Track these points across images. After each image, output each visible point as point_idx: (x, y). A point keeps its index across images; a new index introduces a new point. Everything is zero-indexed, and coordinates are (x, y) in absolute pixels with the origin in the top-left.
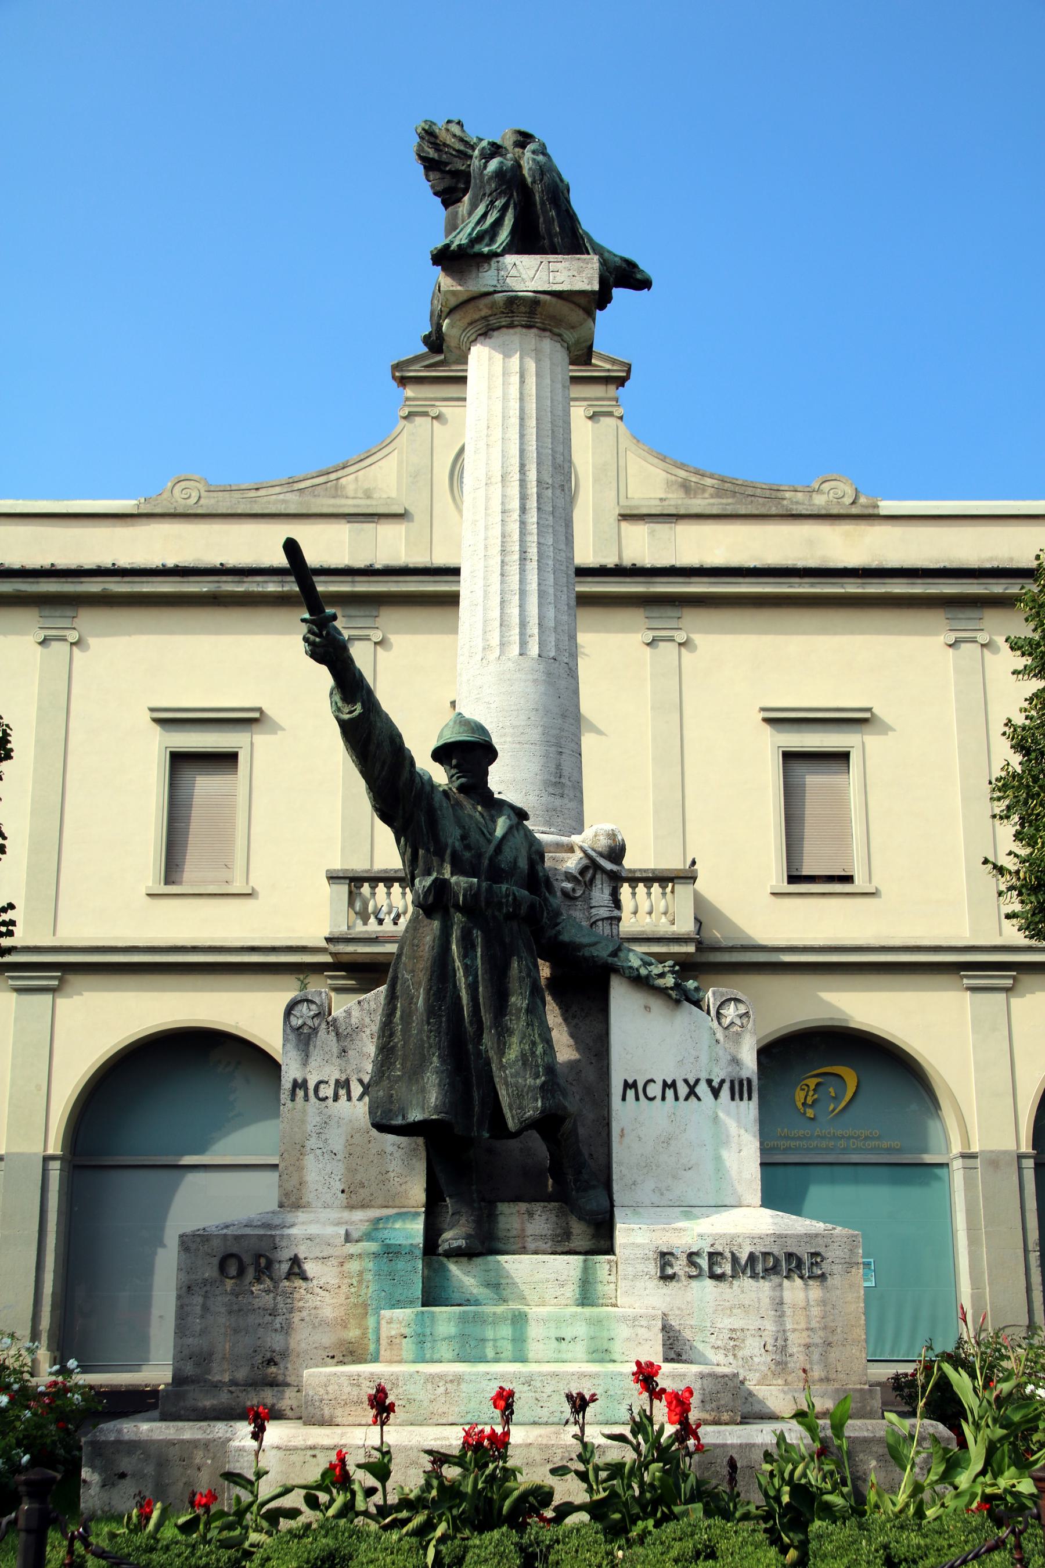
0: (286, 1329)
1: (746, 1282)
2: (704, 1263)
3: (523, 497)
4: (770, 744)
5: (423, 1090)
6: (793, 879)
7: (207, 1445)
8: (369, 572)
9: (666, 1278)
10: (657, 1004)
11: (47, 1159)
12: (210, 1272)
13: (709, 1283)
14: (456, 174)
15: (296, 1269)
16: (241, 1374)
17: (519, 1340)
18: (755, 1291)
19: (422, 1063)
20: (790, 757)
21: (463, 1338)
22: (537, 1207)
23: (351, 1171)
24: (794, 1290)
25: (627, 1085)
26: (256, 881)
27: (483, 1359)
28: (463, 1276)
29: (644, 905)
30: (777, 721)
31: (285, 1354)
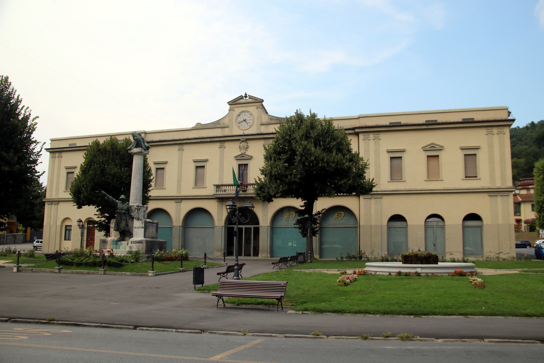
18: (138, 244)
28: (119, 243)
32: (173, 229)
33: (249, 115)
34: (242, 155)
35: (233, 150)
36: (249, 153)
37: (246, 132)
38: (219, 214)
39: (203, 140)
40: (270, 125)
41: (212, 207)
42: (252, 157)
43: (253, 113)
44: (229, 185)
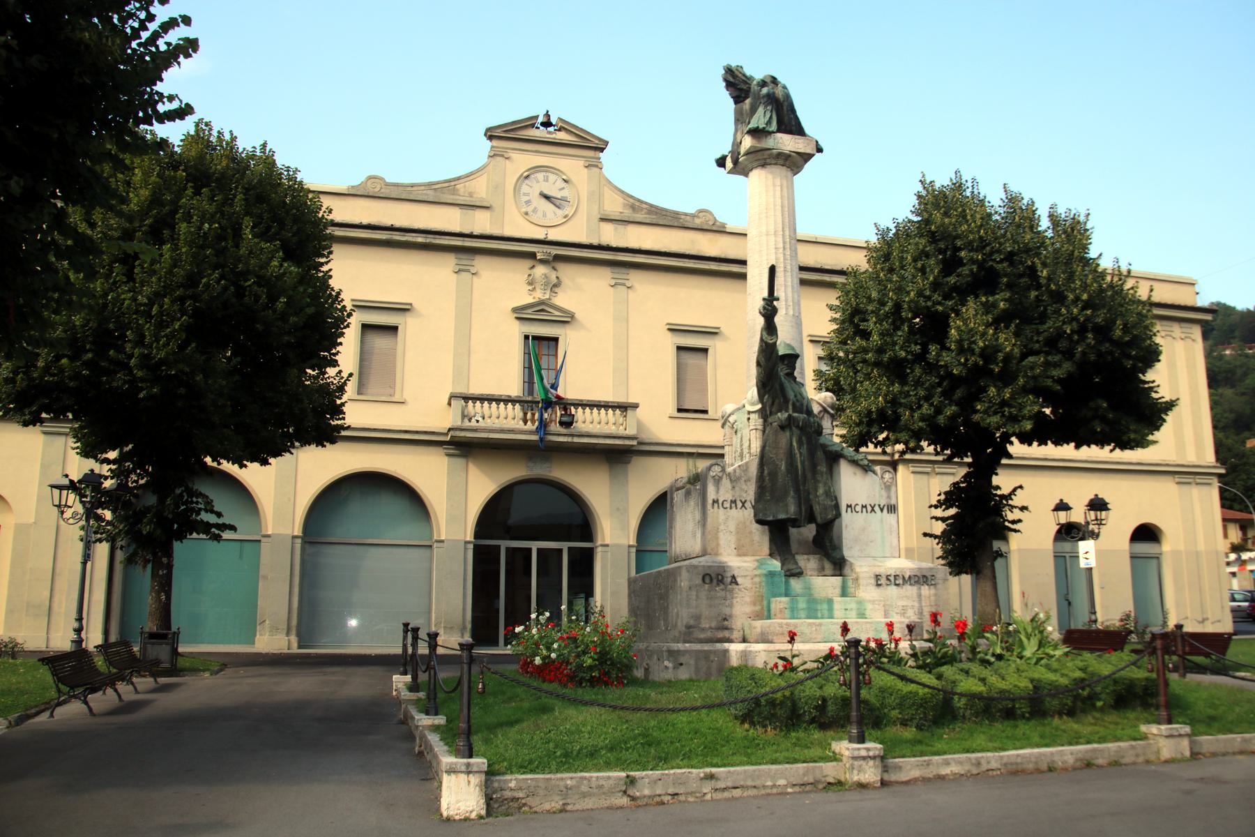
0: (731, 606)
1: (908, 587)
2: (892, 579)
3: (784, 243)
4: (672, 341)
5: (787, 505)
6: (680, 410)
7: (715, 652)
8: (471, 236)
9: (878, 585)
10: (859, 472)
11: (294, 537)
12: (699, 581)
13: (895, 587)
14: (741, 90)
15: (734, 580)
16: (714, 624)
17: (831, 610)
18: (910, 590)
19: (786, 493)
20: (680, 348)
21: (809, 609)
22: (811, 557)
23: (738, 540)
24: (925, 590)
25: (848, 506)
26: (407, 396)
27: (816, 618)
29: (612, 420)
30: (673, 330)
31: (731, 616)
32: (265, 546)
33: (560, 184)
34: (541, 306)
35: (506, 286)
36: (563, 300)
37: (554, 235)
38: (457, 497)
39: (397, 237)
40: (631, 228)
41: (427, 472)
42: (573, 317)
43: (573, 178)
44: (507, 400)
